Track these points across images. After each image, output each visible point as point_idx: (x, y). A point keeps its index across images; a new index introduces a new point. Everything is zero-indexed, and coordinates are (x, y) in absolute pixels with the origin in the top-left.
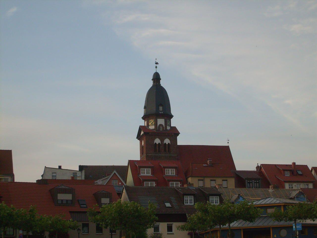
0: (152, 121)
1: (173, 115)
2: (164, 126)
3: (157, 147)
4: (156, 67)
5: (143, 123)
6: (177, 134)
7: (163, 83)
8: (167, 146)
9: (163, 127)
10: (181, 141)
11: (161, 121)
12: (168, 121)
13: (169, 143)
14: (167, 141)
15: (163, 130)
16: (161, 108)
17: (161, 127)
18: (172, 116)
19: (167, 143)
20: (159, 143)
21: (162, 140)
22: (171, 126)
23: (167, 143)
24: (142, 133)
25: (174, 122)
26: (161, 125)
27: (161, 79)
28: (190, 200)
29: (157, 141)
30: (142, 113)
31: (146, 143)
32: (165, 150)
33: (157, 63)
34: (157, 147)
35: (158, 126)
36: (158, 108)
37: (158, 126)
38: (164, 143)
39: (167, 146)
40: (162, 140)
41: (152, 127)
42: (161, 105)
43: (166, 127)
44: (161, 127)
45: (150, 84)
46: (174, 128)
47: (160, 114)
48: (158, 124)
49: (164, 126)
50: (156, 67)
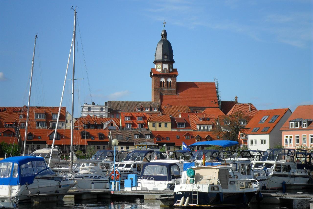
0: (159, 66)
3: (162, 84)
7: (168, 38)
8: (169, 83)
11: (166, 66)
13: (170, 82)
14: (170, 80)
15: (167, 72)
18: (174, 62)
20: (164, 81)
21: (166, 80)
22: (174, 68)
25: (175, 66)
26: (165, 69)
28: (137, 137)
29: (163, 80)
31: (155, 80)
32: (168, 87)
34: (162, 84)
39: (169, 83)
41: (159, 70)
42: (165, 55)
45: (160, 38)
46: (175, 70)
48: (164, 68)
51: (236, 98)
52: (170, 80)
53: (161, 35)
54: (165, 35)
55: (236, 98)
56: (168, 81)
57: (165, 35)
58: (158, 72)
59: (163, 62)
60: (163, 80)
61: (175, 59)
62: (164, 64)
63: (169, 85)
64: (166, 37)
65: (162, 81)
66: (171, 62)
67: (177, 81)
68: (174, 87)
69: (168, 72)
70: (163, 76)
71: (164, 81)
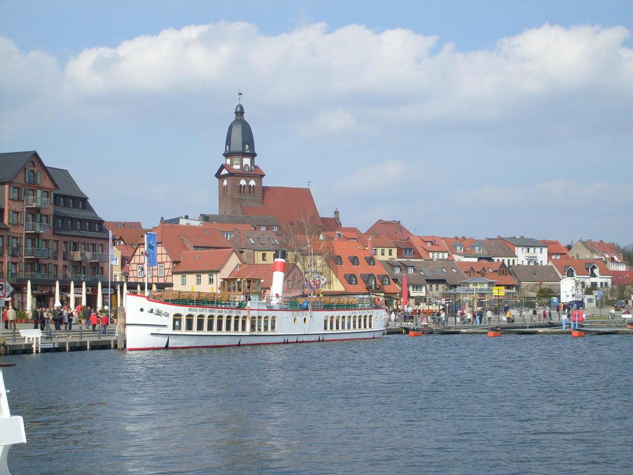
0: (236, 160)
6: (263, 176)
7: (247, 117)
9: (248, 168)
10: (266, 182)
11: (247, 161)
13: (254, 185)
14: (252, 183)
15: (248, 170)
16: (247, 147)
21: (248, 182)
24: (224, 172)
26: (246, 165)
29: (243, 182)
32: (250, 193)
33: (240, 94)
34: (242, 188)
36: (244, 147)
39: (252, 189)
40: (248, 182)
41: (237, 167)
42: (247, 143)
45: (233, 117)
46: (256, 167)
47: (246, 153)
51: (336, 213)
52: (252, 183)
54: (240, 113)
55: (336, 213)
57: (240, 113)
58: (234, 169)
59: (244, 155)
60: (243, 182)
61: (256, 151)
63: (252, 191)
64: (243, 116)
65: (243, 185)
66: (253, 155)
67: (263, 185)
68: (259, 193)
69: (250, 171)
70: (244, 176)
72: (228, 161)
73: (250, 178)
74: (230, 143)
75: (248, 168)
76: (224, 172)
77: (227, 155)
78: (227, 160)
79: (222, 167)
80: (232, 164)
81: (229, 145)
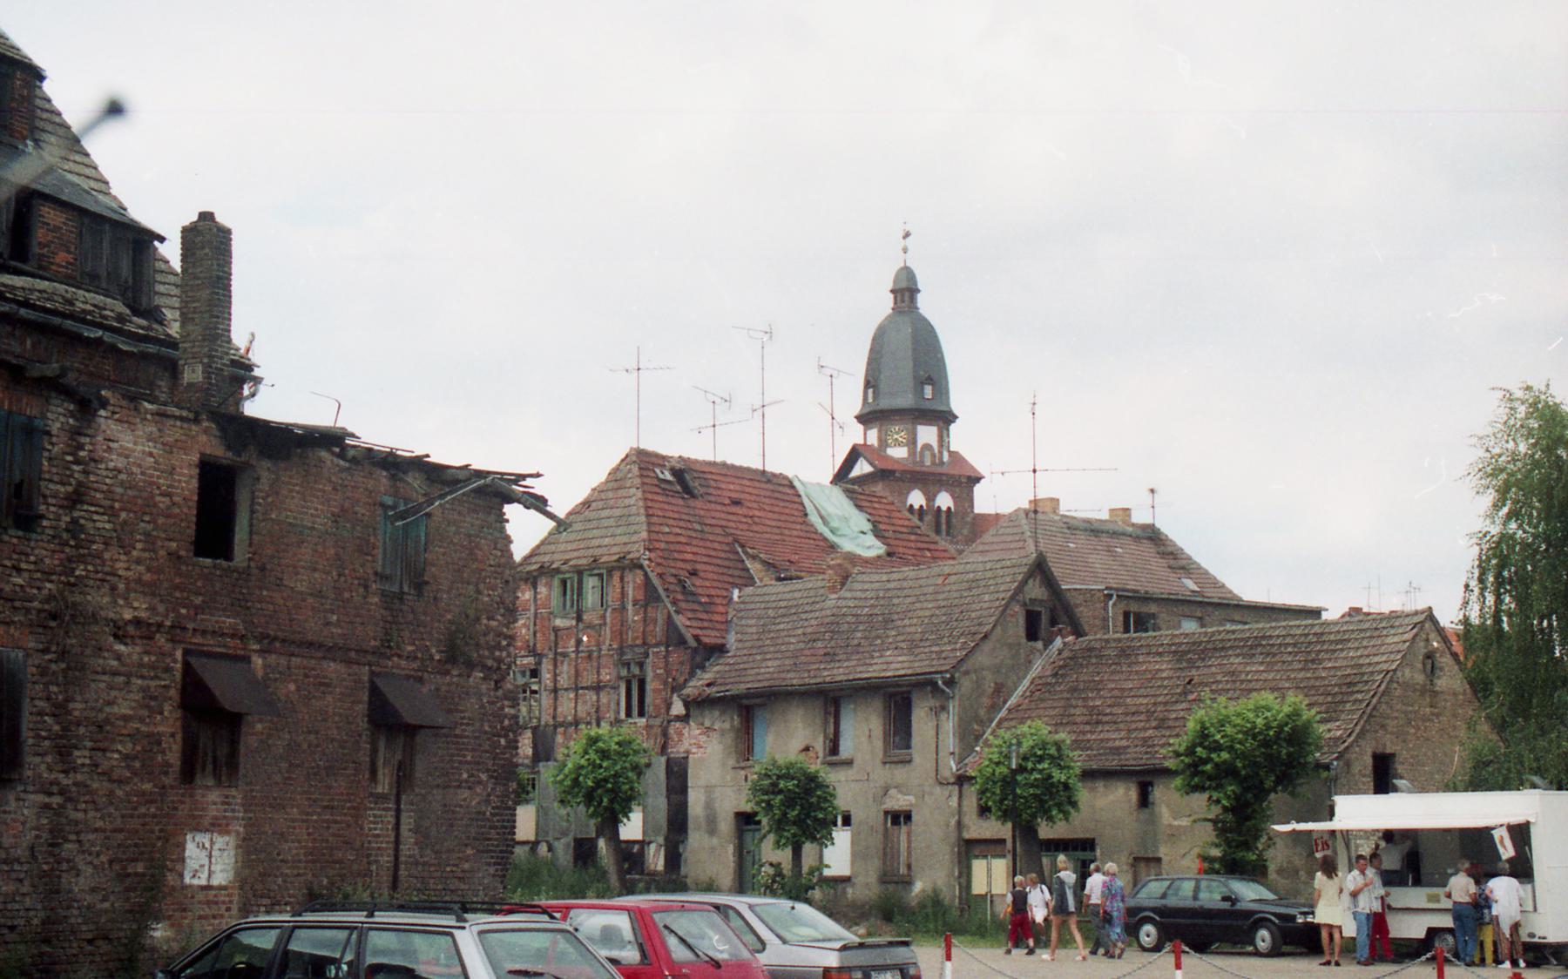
0: (898, 432)
1: (956, 411)
2: (936, 451)
4: (905, 251)
5: (857, 434)
8: (944, 516)
9: (933, 456)
11: (927, 434)
12: (945, 432)
13: (949, 508)
14: (944, 501)
15: (933, 463)
17: (927, 454)
19: (944, 508)
21: (931, 498)
22: (952, 449)
23: (944, 508)
25: (961, 439)
26: (927, 447)
27: (918, 291)
29: (916, 499)
30: (852, 399)
35: (919, 449)
37: (919, 449)
38: (936, 505)
39: (944, 516)
40: (931, 498)
41: (899, 453)
42: (930, 380)
43: (941, 453)
44: (927, 454)
45: (886, 304)
46: (955, 456)
49: (936, 451)
50: (905, 251)
53: (892, 291)
54: (906, 291)
56: (939, 507)
57: (906, 291)
60: (916, 499)
61: (956, 405)
62: (920, 424)
66: (944, 418)
71: (921, 506)
72: (873, 437)
73: (932, 488)
74: (877, 379)
75: (933, 456)
76: (862, 468)
77: (865, 419)
78: (869, 432)
79: (854, 455)
80: (883, 443)
81: (875, 387)
